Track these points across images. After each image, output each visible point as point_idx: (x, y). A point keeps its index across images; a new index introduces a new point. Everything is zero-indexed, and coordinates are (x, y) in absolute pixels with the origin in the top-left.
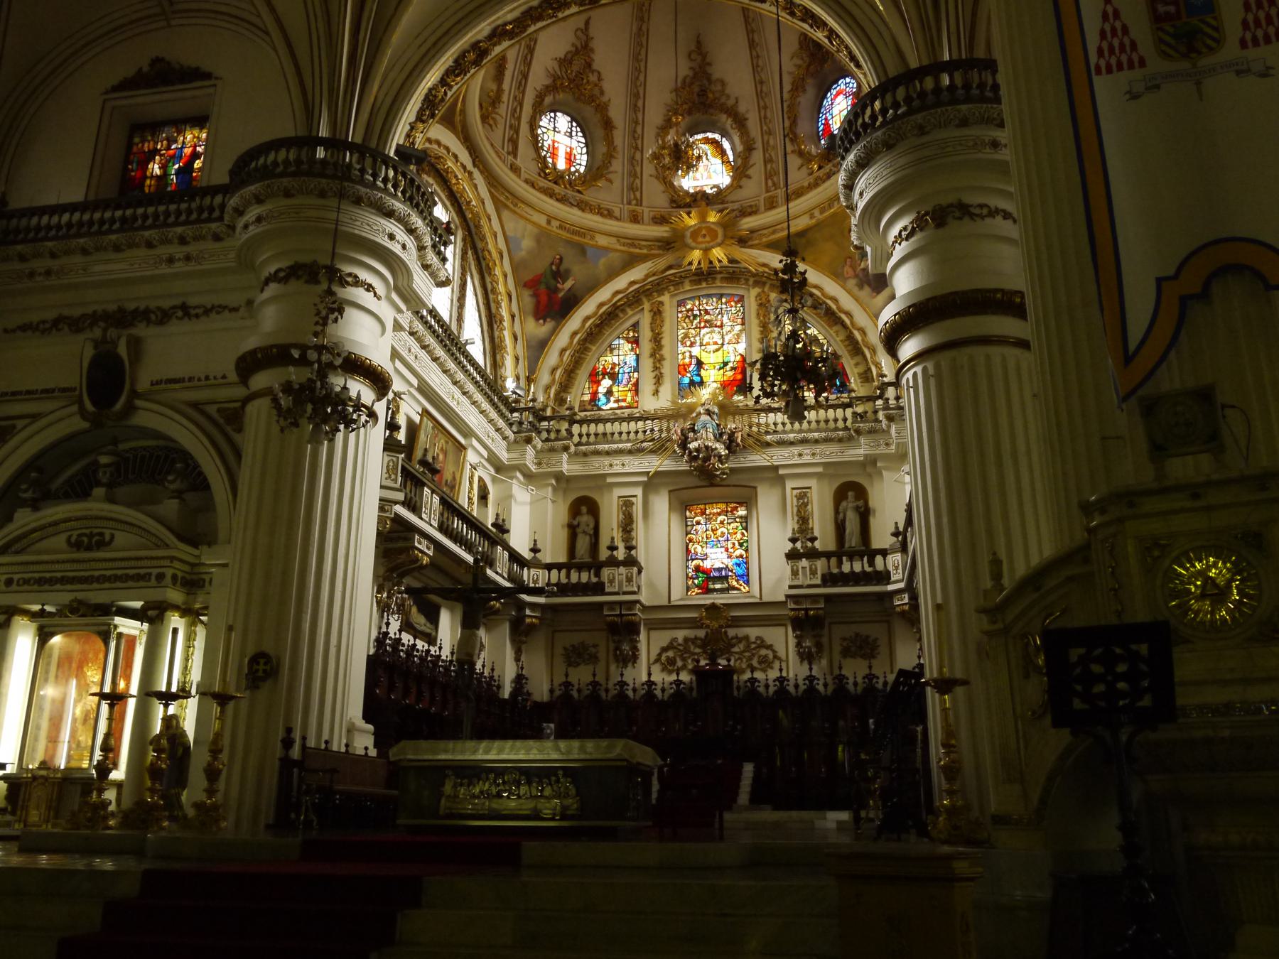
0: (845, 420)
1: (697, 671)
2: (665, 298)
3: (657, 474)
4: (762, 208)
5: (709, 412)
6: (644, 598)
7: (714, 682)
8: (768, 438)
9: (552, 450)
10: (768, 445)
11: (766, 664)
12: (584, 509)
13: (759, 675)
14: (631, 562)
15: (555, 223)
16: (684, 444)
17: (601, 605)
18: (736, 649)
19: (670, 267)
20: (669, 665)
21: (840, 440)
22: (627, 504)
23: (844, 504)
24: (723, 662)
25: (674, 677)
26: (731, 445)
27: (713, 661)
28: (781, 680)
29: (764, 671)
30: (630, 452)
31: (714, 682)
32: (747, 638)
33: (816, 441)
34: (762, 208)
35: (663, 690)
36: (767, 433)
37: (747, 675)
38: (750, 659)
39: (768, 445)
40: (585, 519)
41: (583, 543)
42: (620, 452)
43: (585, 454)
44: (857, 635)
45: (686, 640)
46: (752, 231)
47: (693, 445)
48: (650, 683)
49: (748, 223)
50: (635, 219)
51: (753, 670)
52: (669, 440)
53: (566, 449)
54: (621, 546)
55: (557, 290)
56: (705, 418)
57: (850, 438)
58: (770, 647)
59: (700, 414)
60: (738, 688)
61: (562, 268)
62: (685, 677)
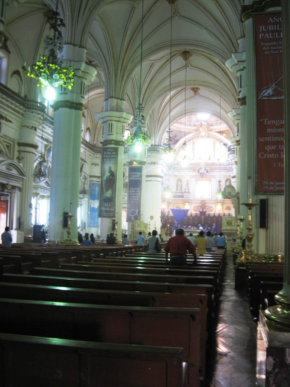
0: (228, 168)
1: (200, 211)
2: (195, 140)
3: (194, 176)
4: (215, 124)
5: (204, 166)
6: (191, 199)
7: (203, 213)
8: (214, 170)
9: (174, 171)
10: (214, 171)
11: (212, 210)
12: (179, 181)
13: (210, 213)
14: (189, 192)
15: (176, 128)
16: (199, 171)
17: (183, 200)
18: (206, 208)
19: (197, 135)
20: (195, 210)
21: (227, 171)
22: (188, 181)
23: (227, 182)
24: (204, 210)
25: (195, 212)
26: (207, 172)
27: (203, 210)
28: (214, 214)
29: (211, 211)
30: (188, 171)
31: (203, 213)
32: (208, 206)
33: (223, 171)
34: (215, 124)
35: (194, 215)
36: (214, 169)
37: (208, 213)
38: (209, 209)
39: (214, 171)
40: (180, 183)
41: (179, 187)
42: (187, 171)
43: (180, 171)
44: (228, 206)
45: (198, 206)
46: (212, 129)
47: (200, 172)
48: (191, 213)
49: (212, 128)
50: (190, 125)
51: (209, 211)
52: (196, 169)
53: (177, 171)
54: (187, 189)
55: (175, 139)
56: (203, 166)
57: (229, 171)
58: (212, 208)
59: (202, 166)
60: (207, 215)
61: (176, 135)
62: (198, 212)
